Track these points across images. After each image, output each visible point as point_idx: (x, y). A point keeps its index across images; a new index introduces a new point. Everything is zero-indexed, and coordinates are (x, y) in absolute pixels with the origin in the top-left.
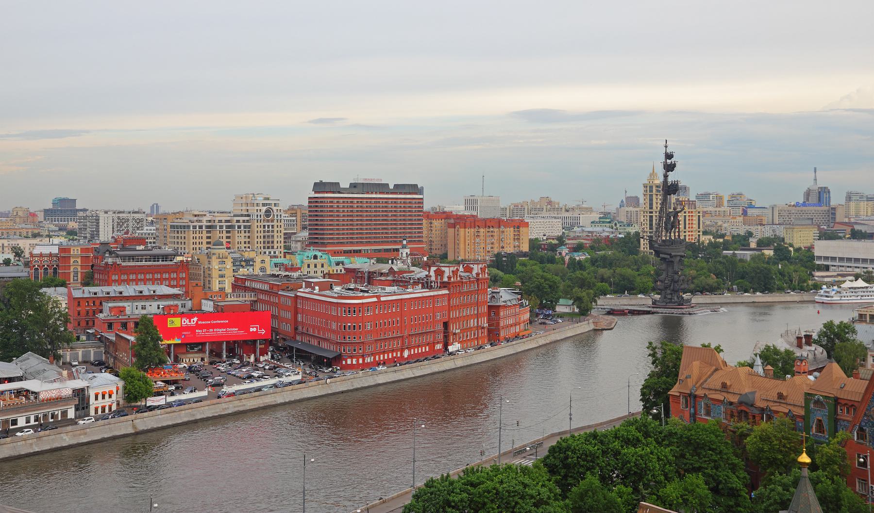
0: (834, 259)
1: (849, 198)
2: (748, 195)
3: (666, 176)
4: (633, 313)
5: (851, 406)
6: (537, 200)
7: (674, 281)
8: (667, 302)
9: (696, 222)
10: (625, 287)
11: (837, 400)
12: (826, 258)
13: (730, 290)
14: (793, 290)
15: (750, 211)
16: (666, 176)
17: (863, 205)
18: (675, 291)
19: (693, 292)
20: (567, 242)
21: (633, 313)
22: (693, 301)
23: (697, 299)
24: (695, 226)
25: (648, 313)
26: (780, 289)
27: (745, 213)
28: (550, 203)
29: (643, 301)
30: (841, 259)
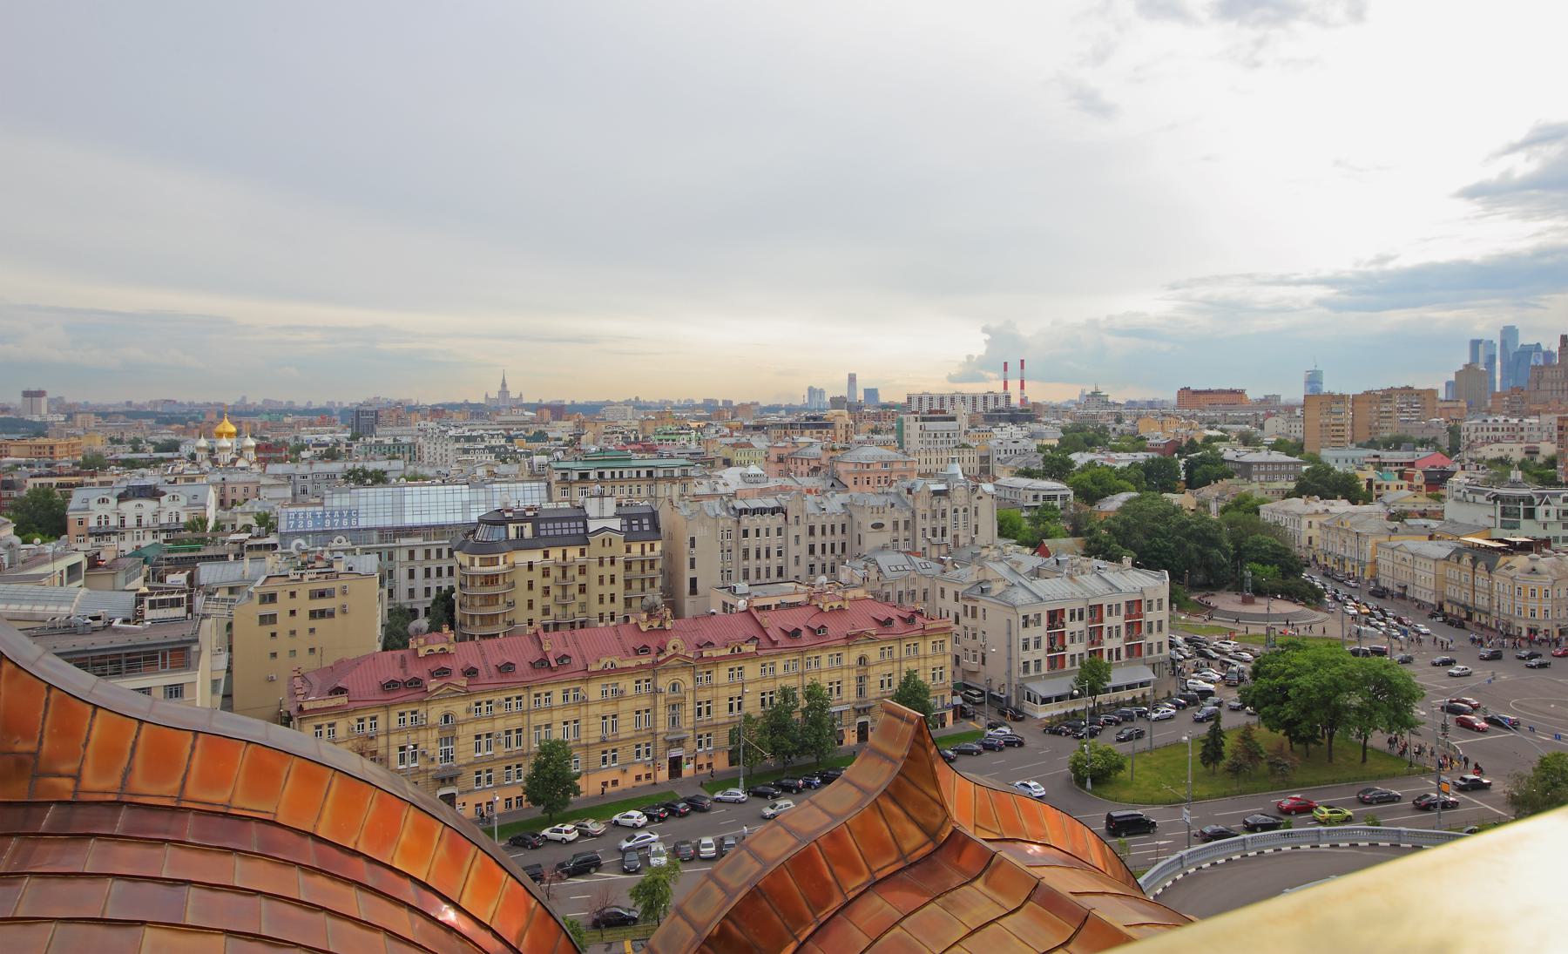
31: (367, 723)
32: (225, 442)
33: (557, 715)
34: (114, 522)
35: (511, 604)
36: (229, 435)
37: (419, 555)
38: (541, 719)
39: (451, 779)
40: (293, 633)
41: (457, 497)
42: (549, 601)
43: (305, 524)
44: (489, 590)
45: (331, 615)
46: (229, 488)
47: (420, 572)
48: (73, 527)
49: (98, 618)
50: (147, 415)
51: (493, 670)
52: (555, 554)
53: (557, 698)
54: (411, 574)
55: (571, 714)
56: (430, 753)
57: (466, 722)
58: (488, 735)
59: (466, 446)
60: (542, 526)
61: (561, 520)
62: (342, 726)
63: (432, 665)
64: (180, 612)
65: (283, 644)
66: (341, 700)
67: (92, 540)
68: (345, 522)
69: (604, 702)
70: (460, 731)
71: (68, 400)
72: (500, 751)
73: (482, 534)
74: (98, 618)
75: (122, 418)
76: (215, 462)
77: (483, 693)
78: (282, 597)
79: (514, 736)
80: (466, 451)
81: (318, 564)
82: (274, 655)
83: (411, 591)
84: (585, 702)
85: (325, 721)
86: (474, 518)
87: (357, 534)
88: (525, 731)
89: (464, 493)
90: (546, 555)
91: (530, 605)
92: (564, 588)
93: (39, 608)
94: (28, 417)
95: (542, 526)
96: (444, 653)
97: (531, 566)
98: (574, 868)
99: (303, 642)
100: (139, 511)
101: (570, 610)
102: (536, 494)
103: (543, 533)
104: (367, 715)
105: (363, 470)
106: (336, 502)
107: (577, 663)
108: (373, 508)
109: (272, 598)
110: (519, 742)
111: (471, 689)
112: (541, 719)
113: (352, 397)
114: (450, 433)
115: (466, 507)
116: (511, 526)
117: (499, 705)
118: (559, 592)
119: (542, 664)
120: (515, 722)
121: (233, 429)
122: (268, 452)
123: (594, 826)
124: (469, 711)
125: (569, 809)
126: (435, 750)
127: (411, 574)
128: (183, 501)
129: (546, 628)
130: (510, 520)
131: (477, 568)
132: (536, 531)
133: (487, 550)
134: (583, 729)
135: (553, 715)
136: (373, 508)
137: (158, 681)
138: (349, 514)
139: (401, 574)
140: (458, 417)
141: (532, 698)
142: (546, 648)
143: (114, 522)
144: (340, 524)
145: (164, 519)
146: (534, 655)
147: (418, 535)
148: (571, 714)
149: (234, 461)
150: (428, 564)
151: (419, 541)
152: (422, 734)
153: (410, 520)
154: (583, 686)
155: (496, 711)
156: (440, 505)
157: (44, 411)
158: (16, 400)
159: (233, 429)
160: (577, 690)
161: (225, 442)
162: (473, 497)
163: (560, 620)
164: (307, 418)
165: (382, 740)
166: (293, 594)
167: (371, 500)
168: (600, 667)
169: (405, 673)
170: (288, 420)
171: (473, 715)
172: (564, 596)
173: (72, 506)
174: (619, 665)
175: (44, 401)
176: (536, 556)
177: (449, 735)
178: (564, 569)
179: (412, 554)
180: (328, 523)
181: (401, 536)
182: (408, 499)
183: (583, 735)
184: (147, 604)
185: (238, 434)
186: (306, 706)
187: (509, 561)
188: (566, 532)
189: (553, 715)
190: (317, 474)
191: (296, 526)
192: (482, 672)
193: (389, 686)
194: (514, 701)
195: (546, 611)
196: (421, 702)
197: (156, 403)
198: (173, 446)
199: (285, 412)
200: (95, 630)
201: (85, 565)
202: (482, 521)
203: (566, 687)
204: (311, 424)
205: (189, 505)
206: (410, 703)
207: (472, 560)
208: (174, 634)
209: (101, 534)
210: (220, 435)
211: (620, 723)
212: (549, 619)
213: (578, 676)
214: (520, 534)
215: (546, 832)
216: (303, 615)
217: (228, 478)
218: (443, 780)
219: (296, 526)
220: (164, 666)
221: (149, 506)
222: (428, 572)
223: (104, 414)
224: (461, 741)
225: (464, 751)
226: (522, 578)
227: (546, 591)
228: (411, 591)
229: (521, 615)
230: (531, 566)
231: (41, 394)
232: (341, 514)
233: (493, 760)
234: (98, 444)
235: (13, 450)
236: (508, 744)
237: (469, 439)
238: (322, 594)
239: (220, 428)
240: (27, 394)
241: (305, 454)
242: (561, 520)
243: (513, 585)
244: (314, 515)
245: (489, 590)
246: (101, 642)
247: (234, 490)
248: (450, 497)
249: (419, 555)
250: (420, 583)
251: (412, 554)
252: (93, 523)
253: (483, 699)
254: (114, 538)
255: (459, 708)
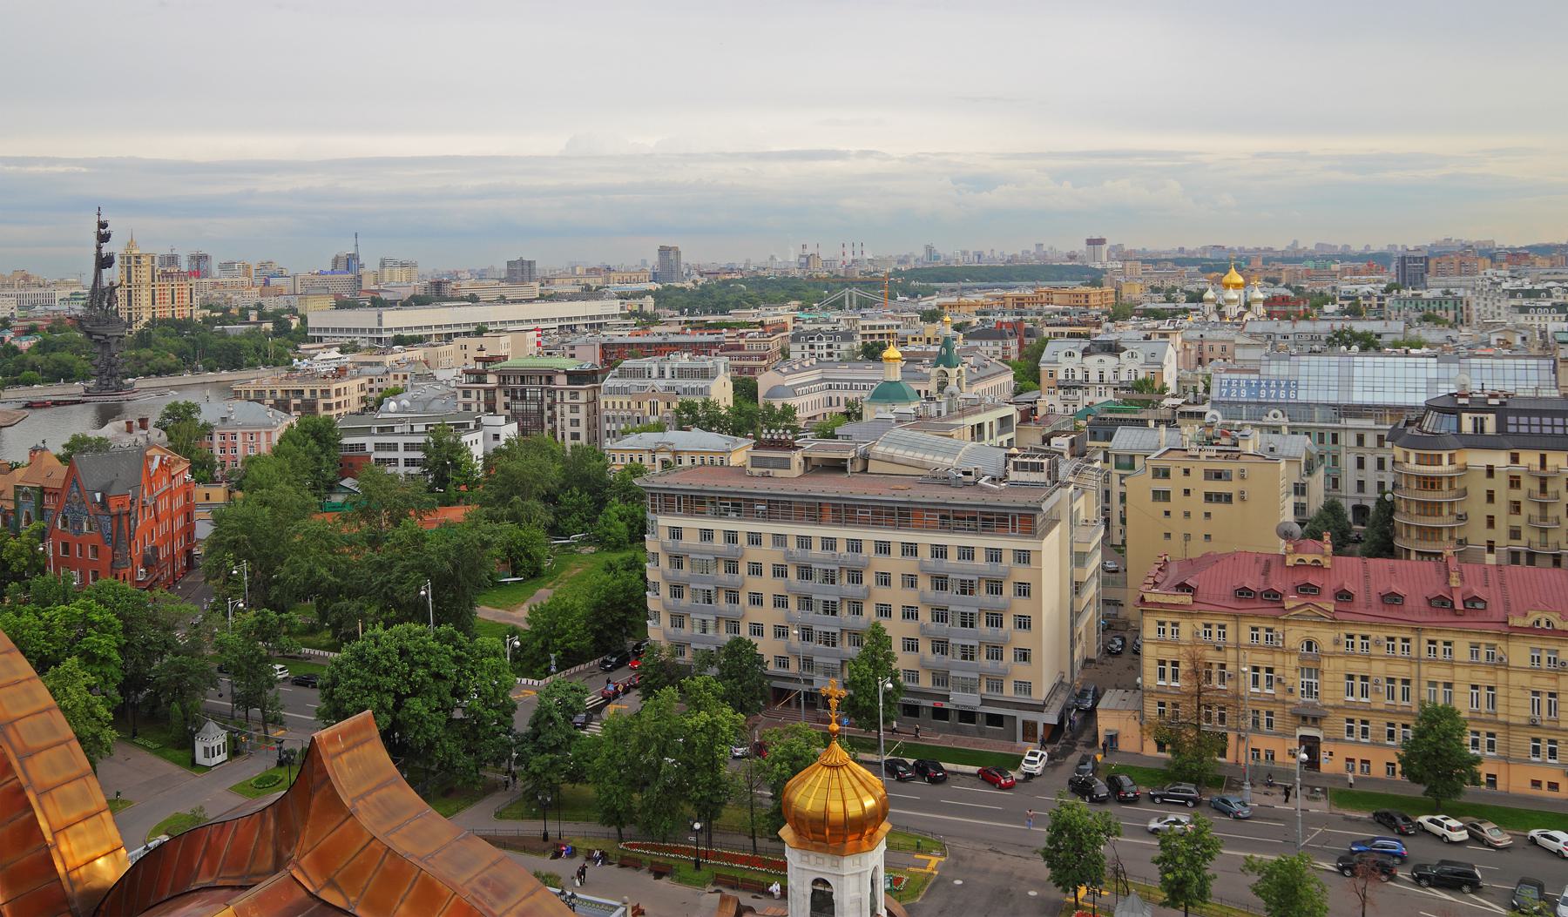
0: (326, 330)
1: (383, 265)
2: (279, 263)
3: (99, 248)
4: (56, 403)
5: (55, 493)
6: (8, 274)
7: (110, 365)
8: (102, 388)
9: (187, 296)
10: (64, 374)
11: (42, 489)
12: (320, 329)
13: (194, 370)
14: (266, 365)
15: (273, 281)
16: (99, 248)
17: (397, 271)
18: (112, 376)
19: (147, 375)
20: (16, 323)
21: (56, 403)
22: (137, 385)
23: (141, 383)
24: (187, 300)
25: (78, 402)
26: (252, 365)
27: (267, 283)
28: (26, 278)
29: (77, 388)
30: (334, 330)
31: (1215, 630)
32: (1232, 294)
33: (1461, 675)
34: (1079, 376)
35: (1462, 518)
36: (1237, 286)
37: (1370, 440)
38: (1440, 673)
39: (1315, 720)
40: (1187, 514)
41: (1421, 373)
42: (1519, 521)
43: (1238, 394)
44: (1430, 496)
45: (1228, 498)
46: (1206, 346)
47: (1371, 462)
48: (1045, 378)
49: (969, 473)
50: (1194, 262)
51: (1375, 599)
52: (1530, 459)
53: (1462, 649)
54: (1361, 463)
55: (1482, 677)
56: (1289, 682)
57: (1331, 656)
58: (1364, 678)
59: (1525, 302)
60: (1512, 419)
61: (1541, 413)
62: (1187, 628)
63: (1299, 578)
64: (1040, 477)
65: (1177, 525)
66: (1186, 599)
67: (1061, 392)
68: (1282, 394)
69: (1535, 671)
70: (1325, 664)
71: (1127, 248)
72: (1381, 702)
73: (1430, 423)
74: (969, 473)
75: (1170, 265)
76: (1222, 316)
77: (1355, 624)
78: (1176, 473)
79: (1399, 686)
80: (1524, 310)
81: (1224, 441)
82: (1168, 535)
83: (1361, 484)
84: (1502, 665)
85: (1169, 619)
86: (1421, 400)
87: (1298, 413)
88: (1414, 683)
89: (1432, 368)
90: (1515, 459)
91: (1491, 522)
92: (1543, 506)
93: (929, 457)
94: (1091, 265)
95: (1512, 419)
96: (1317, 566)
97: (1490, 471)
98: (1438, 877)
99: (1198, 526)
100: (1101, 366)
101: (1552, 538)
102: (1533, 375)
103: (1512, 429)
104: (1216, 621)
105: (1351, 331)
106: (1273, 370)
107: (1496, 610)
108: (1320, 379)
109: (1166, 474)
110: (1406, 695)
111: (1339, 616)
112: (1440, 673)
113: (1415, 237)
114: (1505, 286)
115: (1431, 383)
116: (1465, 416)
117: (1377, 643)
118: (1535, 511)
119: (1442, 603)
120: (1400, 670)
121: (1241, 280)
122: (1276, 307)
123: (1490, 831)
124: (1337, 642)
125: (1463, 799)
126: (1296, 680)
127: (1361, 463)
128: (1141, 359)
129: (1515, 557)
130: (1465, 408)
131: (1412, 466)
132: (1501, 425)
133: (1429, 445)
134: (1500, 700)
135: (1459, 674)
136: (1320, 379)
137: (1008, 543)
138: (1288, 385)
139: (1348, 461)
140: (1542, 264)
141: (1425, 645)
142: (1455, 582)
143: (1079, 376)
144: (1277, 396)
145: (1124, 377)
146: (1435, 589)
147: (1368, 416)
148: (1482, 677)
149: (1241, 315)
150: (1381, 453)
151: (1369, 423)
152: (1278, 658)
153: (1358, 398)
154: (1501, 644)
155: (1373, 650)
156: (1398, 380)
157: (1105, 258)
158: (1080, 247)
159: (1241, 280)
160: (1493, 646)
161: (1232, 294)
162: (1443, 374)
163: (1536, 548)
164: (1351, 265)
165: (1231, 654)
166: (1187, 472)
167: (1313, 370)
168: (1529, 622)
169: (1266, 582)
170: (1336, 267)
171: (1343, 648)
172: (1544, 518)
173: (1044, 358)
174: (1559, 625)
175: (1105, 248)
176: (1501, 460)
177: (1312, 665)
178: (1543, 482)
179: (1360, 440)
180: (1263, 393)
181: (1346, 416)
182: (1357, 372)
183: (1500, 709)
184: (1011, 465)
185: (1245, 285)
186: (1148, 598)
187: (1459, 460)
188: (1547, 430)
189: (1459, 674)
190: (1300, 334)
191: (1228, 395)
192: (1360, 598)
193: (1243, 593)
194: (1399, 644)
195: (1515, 534)
196: (1276, 619)
197: (1205, 249)
198: (1197, 297)
199: (1332, 259)
200: (966, 484)
201: (1017, 418)
202: (1429, 407)
203: (1476, 639)
204: (1356, 272)
205: (1147, 363)
206: (1263, 618)
207: (1407, 454)
208: (1022, 499)
209: (1068, 387)
210: (1227, 286)
211: (1561, 707)
212: (1520, 545)
213: (1492, 629)
214: (1479, 426)
215: (1423, 819)
216: (1198, 496)
217: (1207, 335)
218: (1305, 718)
219: (1228, 395)
220: (1014, 530)
221: (1110, 361)
222: (1381, 464)
223: (1153, 261)
224: (1327, 676)
225: (1332, 689)
226: (1479, 486)
227: (1516, 507)
228: (1361, 484)
229: (1478, 535)
230: (1490, 471)
231: (1101, 241)
232: (1278, 385)
233: (1368, 709)
234: (1135, 292)
235: (1056, 298)
236: (1391, 694)
237: (1528, 294)
238: (1218, 476)
239: (1226, 279)
240: (1090, 242)
241: (1329, 308)
242: (1541, 413)
243: (1465, 492)
244: (1248, 383)
245: (1430, 496)
246: (960, 497)
247: (1212, 349)
248: (1411, 372)
249: (1370, 440)
250: (1371, 475)
251: (1360, 440)
252: (1061, 376)
253: (1359, 632)
254: (1079, 393)
255: (1325, 637)
